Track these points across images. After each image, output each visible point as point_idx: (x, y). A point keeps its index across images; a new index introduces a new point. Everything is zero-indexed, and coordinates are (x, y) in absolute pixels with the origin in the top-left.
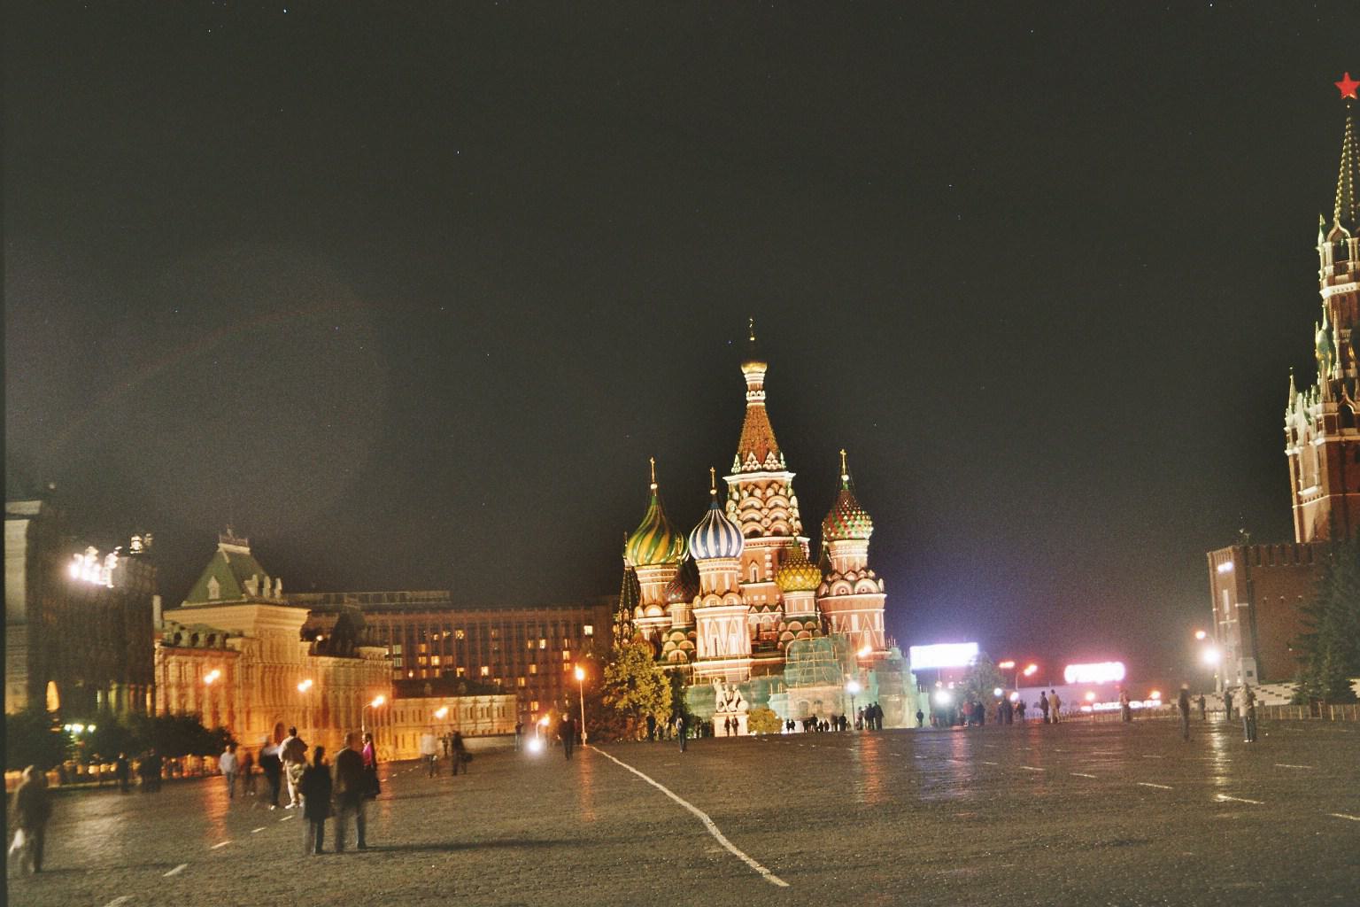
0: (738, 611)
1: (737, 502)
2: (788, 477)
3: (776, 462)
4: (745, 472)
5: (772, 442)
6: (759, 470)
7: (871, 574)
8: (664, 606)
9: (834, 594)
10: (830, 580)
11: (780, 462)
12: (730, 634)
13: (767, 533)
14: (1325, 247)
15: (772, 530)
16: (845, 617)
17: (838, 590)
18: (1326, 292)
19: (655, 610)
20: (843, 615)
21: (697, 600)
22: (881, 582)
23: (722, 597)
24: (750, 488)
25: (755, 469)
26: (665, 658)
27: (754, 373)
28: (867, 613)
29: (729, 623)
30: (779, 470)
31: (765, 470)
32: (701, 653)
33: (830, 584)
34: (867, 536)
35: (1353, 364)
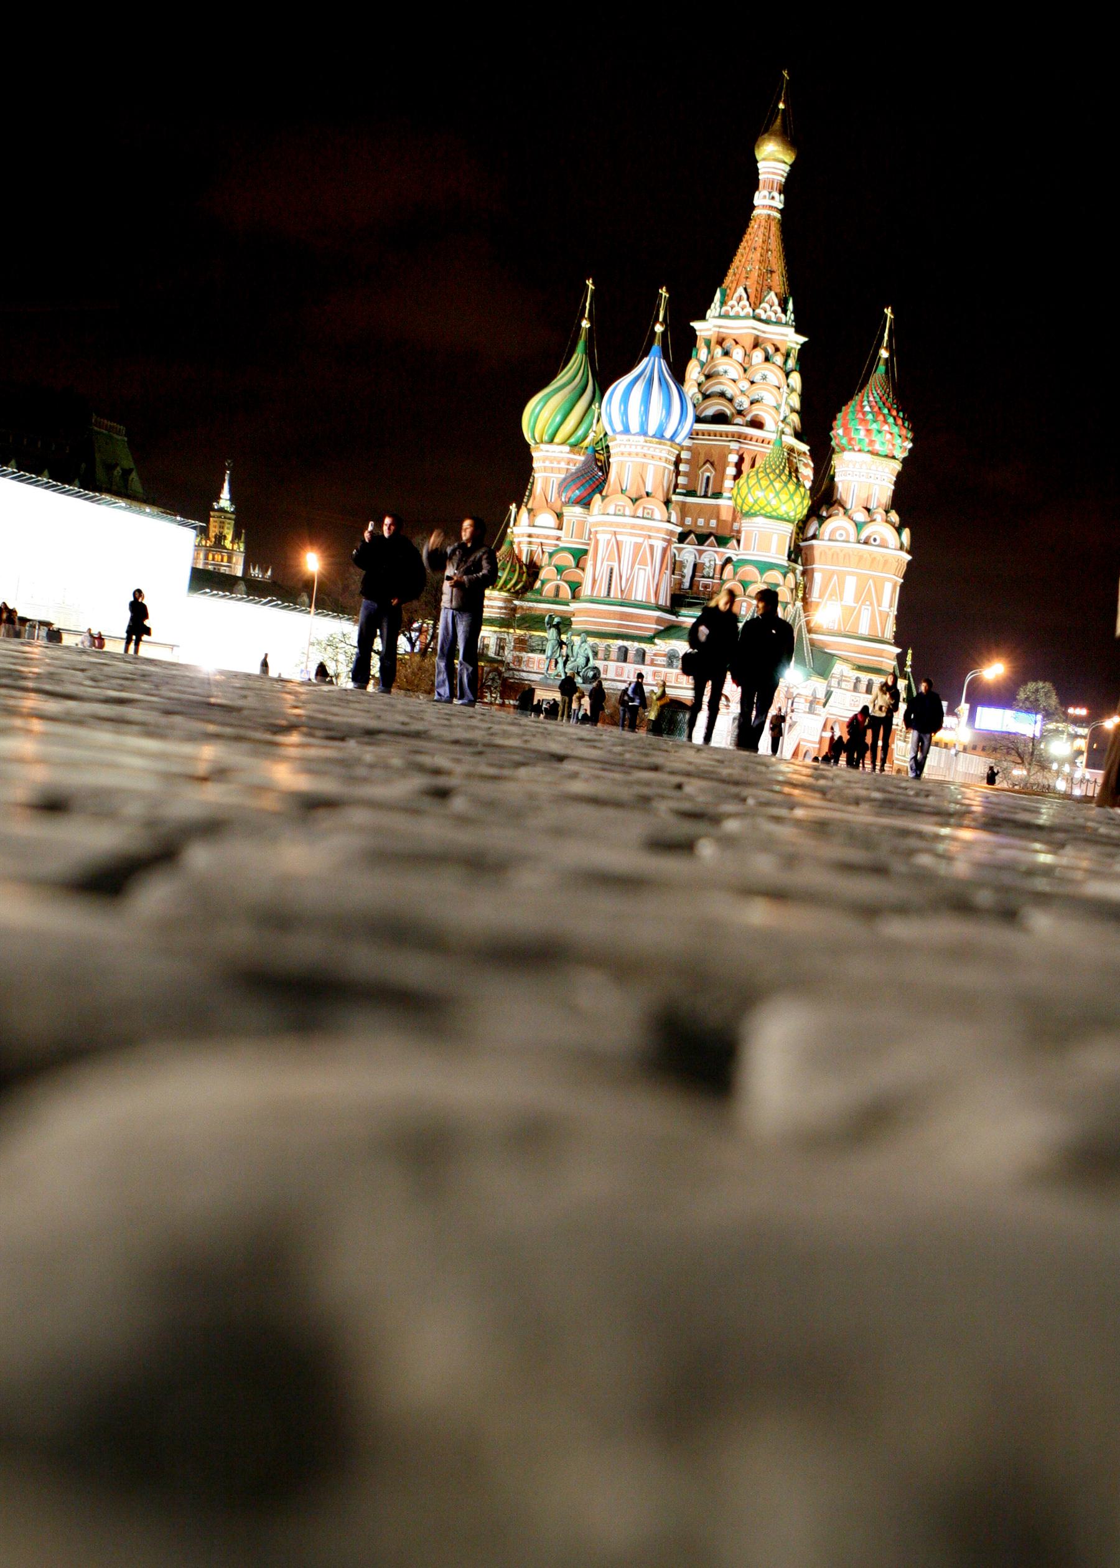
0: (658, 530)
1: (702, 365)
2: (795, 340)
3: (779, 310)
4: (726, 316)
5: (778, 280)
6: (746, 317)
7: (894, 517)
9: (826, 538)
10: (824, 514)
11: (784, 311)
12: (637, 566)
13: (739, 420)
15: (748, 418)
16: (835, 577)
17: (833, 532)
20: (833, 572)
22: (906, 533)
23: (634, 501)
24: (726, 344)
25: (742, 314)
26: (540, 592)
27: (773, 160)
28: (872, 577)
29: (637, 547)
30: (778, 323)
32: (586, 590)
33: (822, 520)
34: (901, 455)
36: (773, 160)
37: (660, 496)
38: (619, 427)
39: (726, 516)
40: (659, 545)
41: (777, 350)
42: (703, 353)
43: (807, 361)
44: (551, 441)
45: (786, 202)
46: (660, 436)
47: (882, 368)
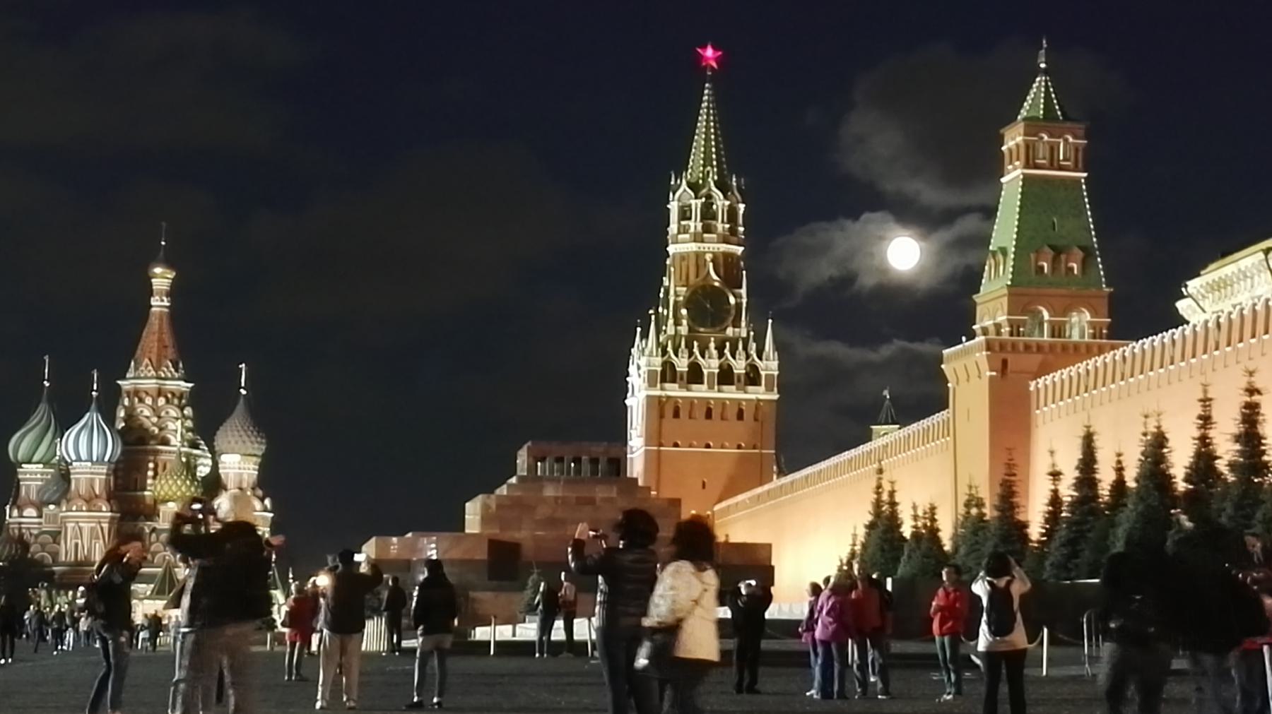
2: (185, 386)
5: (170, 352)
6: (151, 378)
7: (260, 493)
8: (40, 506)
11: (177, 371)
14: (674, 207)
18: (672, 249)
19: (30, 512)
21: (64, 502)
22: (267, 502)
27: (162, 278)
31: (159, 378)
34: (260, 453)
35: (685, 322)
36: (162, 278)
37: (104, 495)
38: (74, 458)
39: (149, 501)
40: (106, 526)
41: (173, 394)
42: (126, 402)
43: (194, 399)
44: (29, 462)
45: (171, 301)
46: (100, 461)
47: (242, 401)
